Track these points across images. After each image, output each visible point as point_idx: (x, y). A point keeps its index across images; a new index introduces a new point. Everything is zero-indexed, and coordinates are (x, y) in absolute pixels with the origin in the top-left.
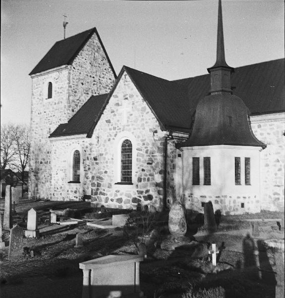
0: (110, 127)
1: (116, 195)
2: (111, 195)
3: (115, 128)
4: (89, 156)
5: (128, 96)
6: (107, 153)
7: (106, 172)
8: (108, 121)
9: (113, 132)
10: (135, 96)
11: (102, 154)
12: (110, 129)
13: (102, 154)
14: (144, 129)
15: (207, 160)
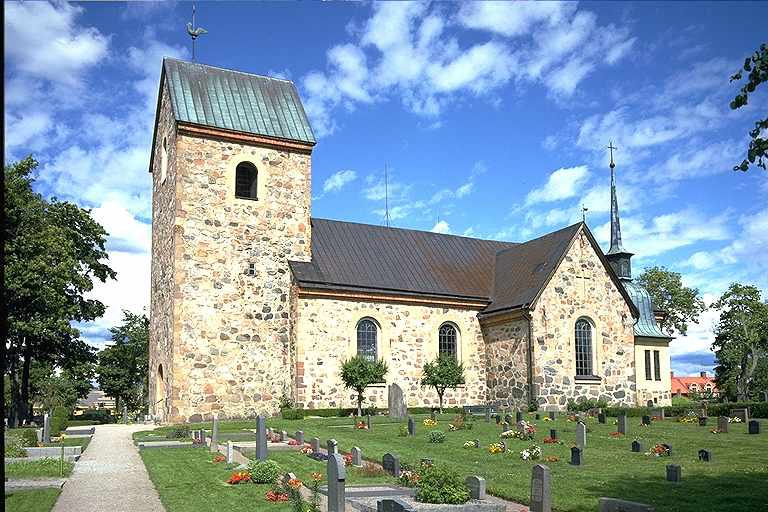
0: (563, 299)
1: (576, 393)
2: (570, 393)
3: (570, 303)
4: (403, 334)
5: (586, 264)
6: (559, 336)
7: (559, 362)
8: (559, 290)
9: (567, 307)
10: (596, 267)
11: (553, 336)
12: (562, 302)
13: (553, 336)
14: (610, 310)
15: (656, 353)
